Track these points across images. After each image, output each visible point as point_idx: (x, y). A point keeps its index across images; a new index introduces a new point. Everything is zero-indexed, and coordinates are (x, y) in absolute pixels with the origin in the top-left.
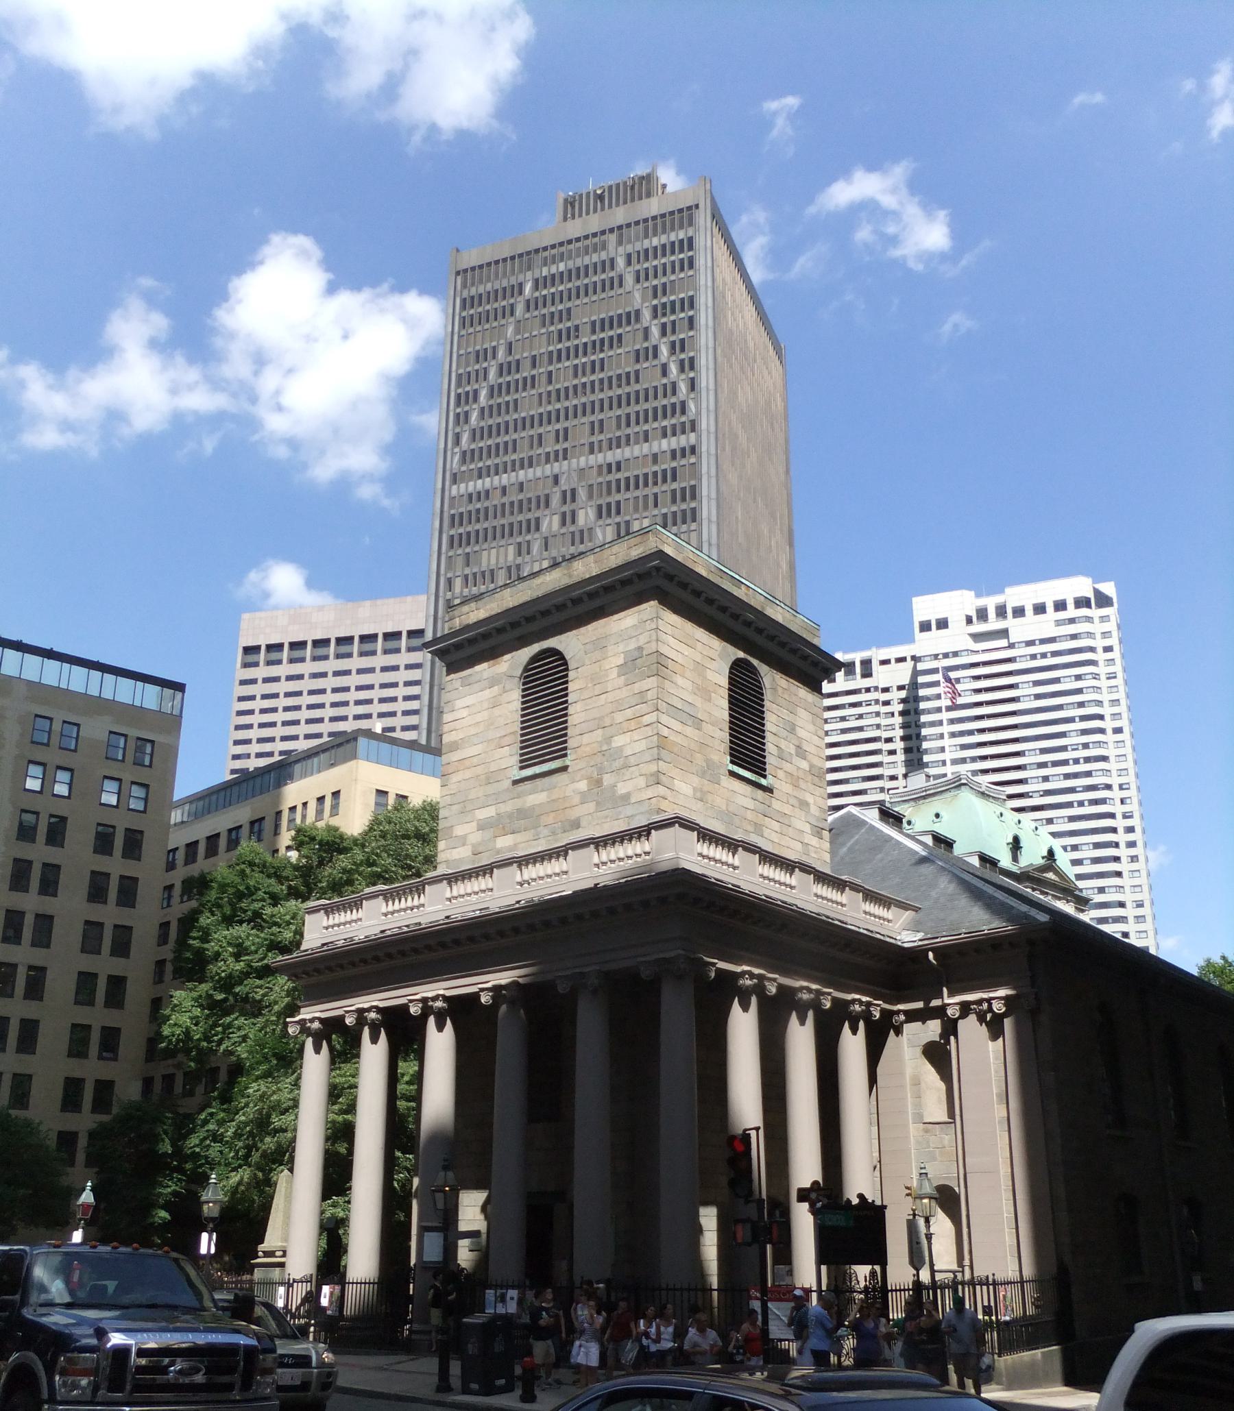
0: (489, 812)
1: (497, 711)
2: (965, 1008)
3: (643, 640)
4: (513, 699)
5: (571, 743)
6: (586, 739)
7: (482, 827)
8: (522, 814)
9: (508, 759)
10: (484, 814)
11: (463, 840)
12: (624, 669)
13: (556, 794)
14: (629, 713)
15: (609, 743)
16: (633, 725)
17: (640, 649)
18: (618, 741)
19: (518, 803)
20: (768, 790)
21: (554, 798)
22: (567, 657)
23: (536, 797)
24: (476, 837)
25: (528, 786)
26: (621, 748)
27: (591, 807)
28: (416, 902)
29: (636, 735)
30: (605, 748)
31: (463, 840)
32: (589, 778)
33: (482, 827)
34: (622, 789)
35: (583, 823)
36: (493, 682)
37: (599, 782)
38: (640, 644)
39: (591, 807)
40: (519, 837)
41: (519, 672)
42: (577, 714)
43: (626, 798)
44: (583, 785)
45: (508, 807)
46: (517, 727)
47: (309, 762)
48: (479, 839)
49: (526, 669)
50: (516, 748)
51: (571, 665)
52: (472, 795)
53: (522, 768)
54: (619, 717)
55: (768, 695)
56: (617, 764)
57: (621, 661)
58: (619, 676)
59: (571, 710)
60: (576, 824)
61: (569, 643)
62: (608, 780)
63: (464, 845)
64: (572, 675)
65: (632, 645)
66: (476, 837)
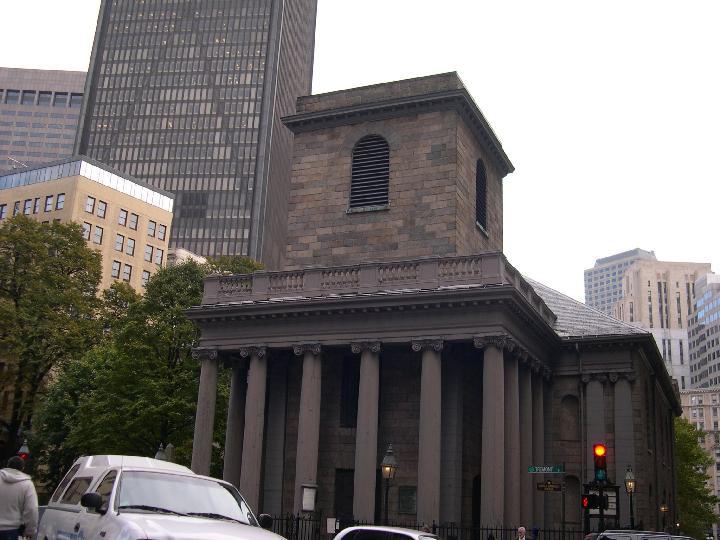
0: (328, 231)
1: (334, 168)
2: (593, 377)
3: (445, 140)
4: (346, 164)
5: (390, 196)
6: (402, 195)
7: (321, 239)
8: (351, 234)
9: (342, 200)
10: (321, 232)
11: (307, 247)
12: (429, 156)
13: (379, 226)
14: (435, 183)
15: (420, 198)
16: (438, 191)
17: (444, 145)
18: (426, 200)
19: (351, 228)
20: (487, 238)
21: (377, 228)
22: (390, 142)
23: (364, 227)
24: (317, 246)
25: (359, 218)
26: (428, 205)
27: (405, 237)
28: (279, 284)
29: (440, 197)
30: (417, 202)
31: (307, 247)
32: (405, 220)
33: (321, 239)
34: (429, 229)
35: (399, 246)
36: (331, 150)
37: (412, 222)
38: (444, 142)
39: (405, 237)
40: (349, 250)
41: (352, 146)
42: (396, 179)
43: (433, 234)
44: (400, 223)
45: (344, 229)
46: (348, 180)
47: (43, 171)
48: (319, 247)
49: (357, 145)
50: (348, 193)
51: (392, 148)
52: (314, 218)
53: (351, 206)
54: (427, 185)
55: (488, 181)
56: (426, 213)
57: (429, 151)
58: (428, 159)
59: (391, 175)
60: (395, 247)
61: (395, 134)
62: (418, 221)
63: (307, 249)
64: (392, 153)
65: (438, 142)
66: (317, 246)
